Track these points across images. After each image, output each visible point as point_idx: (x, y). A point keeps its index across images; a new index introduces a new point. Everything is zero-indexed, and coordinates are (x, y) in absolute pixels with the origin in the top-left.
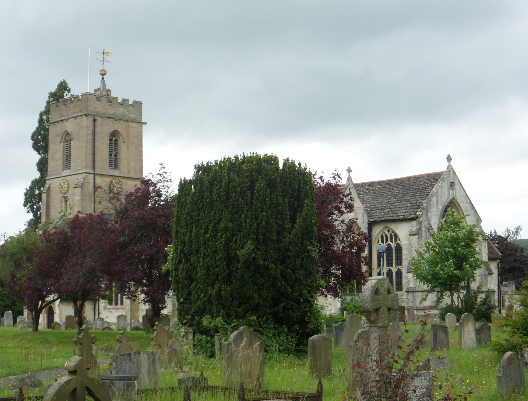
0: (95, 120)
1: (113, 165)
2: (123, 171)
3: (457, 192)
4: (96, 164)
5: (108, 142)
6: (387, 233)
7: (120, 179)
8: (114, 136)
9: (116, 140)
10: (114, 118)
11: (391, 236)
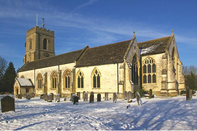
6: (148, 59)
8: (45, 40)
11: (150, 61)
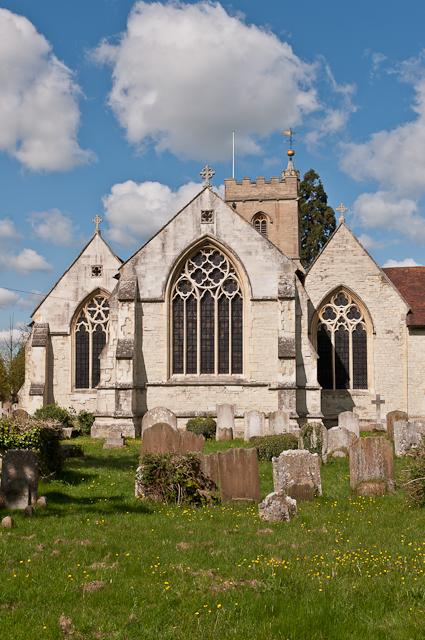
3: (221, 227)
9: (264, 222)
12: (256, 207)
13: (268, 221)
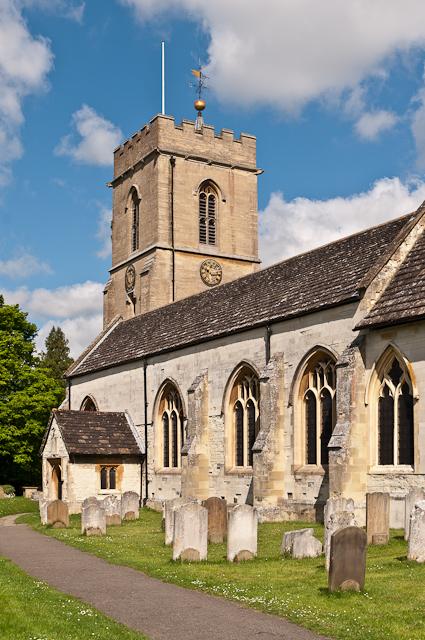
0: (172, 162)
1: (207, 241)
2: (223, 247)
4: (176, 235)
5: (197, 198)
7: (218, 260)
9: (212, 198)
10: (205, 160)
12: (205, 172)
13: (218, 200)
